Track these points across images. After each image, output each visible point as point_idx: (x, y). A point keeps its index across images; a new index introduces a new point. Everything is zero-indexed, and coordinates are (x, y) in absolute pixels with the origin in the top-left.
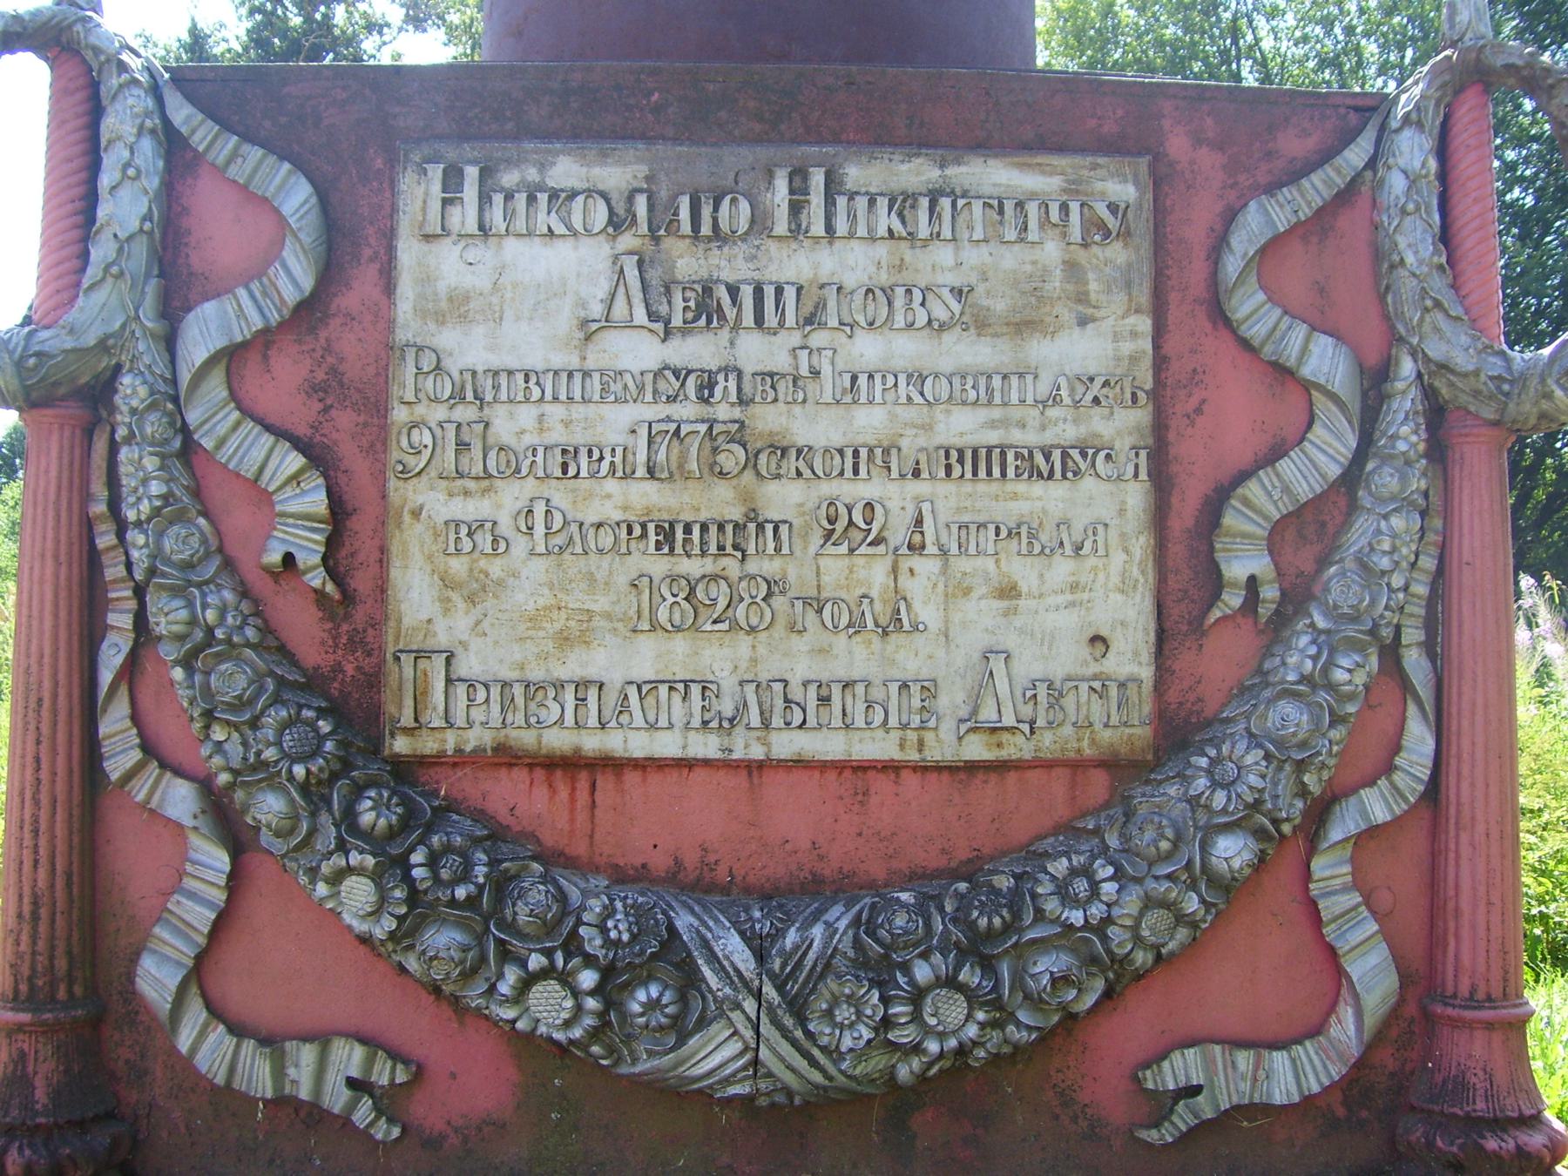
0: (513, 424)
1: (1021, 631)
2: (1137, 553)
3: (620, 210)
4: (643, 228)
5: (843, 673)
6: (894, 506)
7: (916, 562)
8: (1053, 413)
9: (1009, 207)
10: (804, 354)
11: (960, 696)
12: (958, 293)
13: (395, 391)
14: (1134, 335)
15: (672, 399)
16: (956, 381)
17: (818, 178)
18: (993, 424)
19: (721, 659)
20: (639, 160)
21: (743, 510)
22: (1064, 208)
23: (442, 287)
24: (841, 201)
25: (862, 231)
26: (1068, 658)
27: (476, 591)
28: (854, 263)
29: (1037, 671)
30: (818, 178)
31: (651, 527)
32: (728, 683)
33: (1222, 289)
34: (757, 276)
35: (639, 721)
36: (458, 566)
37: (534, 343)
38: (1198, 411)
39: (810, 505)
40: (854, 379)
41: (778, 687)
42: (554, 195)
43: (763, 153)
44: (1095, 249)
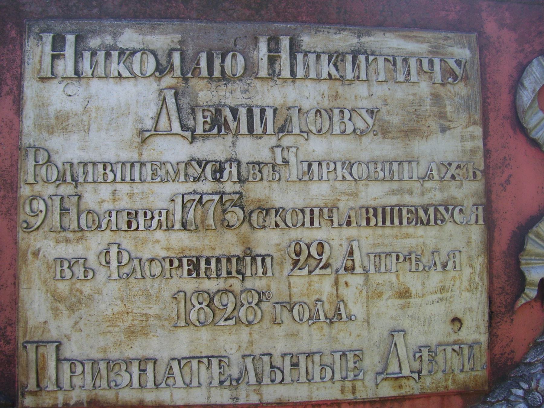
0: (97, 196)
1: (412, 318)
2: (478, 267)
3: (163, 62)
4: (178, 73)
5: (305, 348)
6: (335, 243)
7: (349, 278)
8: (428, 185)
9: (399, 61)
10: (278, 151)
11: (377, 359)
12: (371, 112)
13: (22, 176)
14: (473, 137)
15: (196, 180)
16: (372, 166)
17: (285, 43)
18: (393, 192)
19: (230, 342)
20: (175, 31)
21: (243, 248)
22: (431, 62)
23: (52, 110)
24: (300, 57)
25: (312, 75)
26: (440, 332)
27: (74, 303)
28: (308, 94)
29: (422, 340)
30: (285, 43)
31: (185, 261)
32: (235, 357)
33: (520, 110)
34: (248, 102)
35: (179, 382)
36: (63, 287)
37: (110, 145)
38: (508, 182)
39: (284, 245)
40: (310, 165)
41: (266, 359)
42: (122, 53)
43: (251, 27)
44: (449, 87)
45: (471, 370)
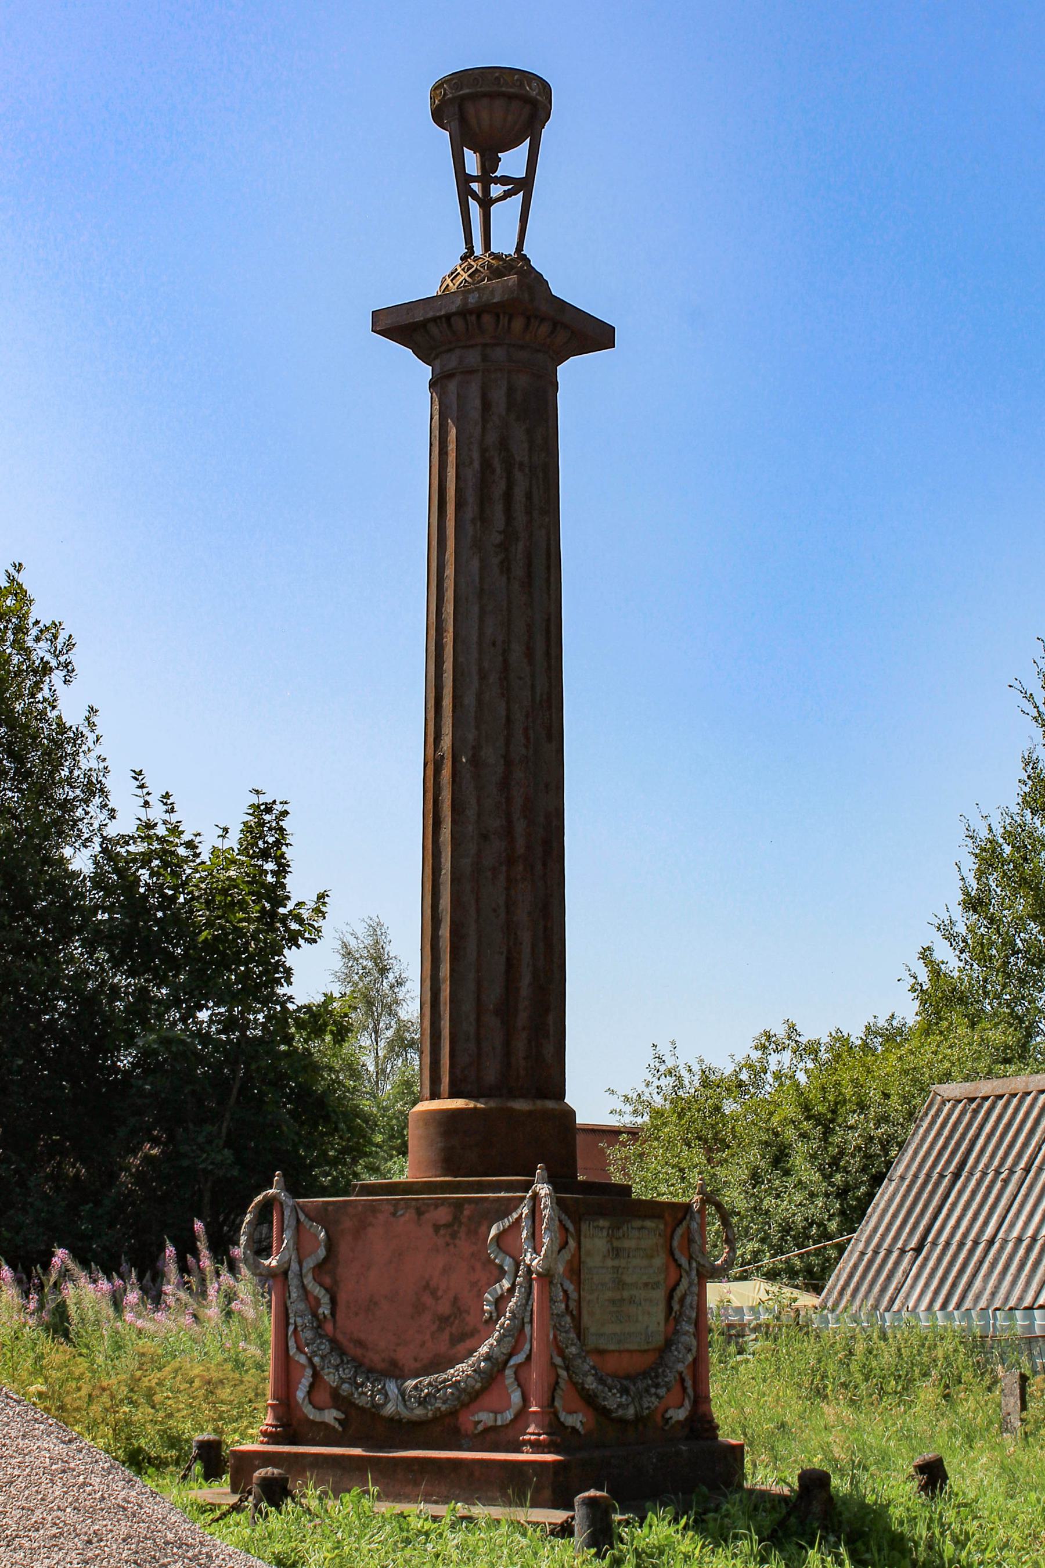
45: (659, 1341)
